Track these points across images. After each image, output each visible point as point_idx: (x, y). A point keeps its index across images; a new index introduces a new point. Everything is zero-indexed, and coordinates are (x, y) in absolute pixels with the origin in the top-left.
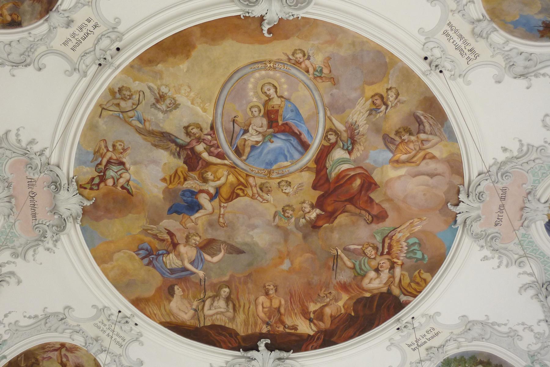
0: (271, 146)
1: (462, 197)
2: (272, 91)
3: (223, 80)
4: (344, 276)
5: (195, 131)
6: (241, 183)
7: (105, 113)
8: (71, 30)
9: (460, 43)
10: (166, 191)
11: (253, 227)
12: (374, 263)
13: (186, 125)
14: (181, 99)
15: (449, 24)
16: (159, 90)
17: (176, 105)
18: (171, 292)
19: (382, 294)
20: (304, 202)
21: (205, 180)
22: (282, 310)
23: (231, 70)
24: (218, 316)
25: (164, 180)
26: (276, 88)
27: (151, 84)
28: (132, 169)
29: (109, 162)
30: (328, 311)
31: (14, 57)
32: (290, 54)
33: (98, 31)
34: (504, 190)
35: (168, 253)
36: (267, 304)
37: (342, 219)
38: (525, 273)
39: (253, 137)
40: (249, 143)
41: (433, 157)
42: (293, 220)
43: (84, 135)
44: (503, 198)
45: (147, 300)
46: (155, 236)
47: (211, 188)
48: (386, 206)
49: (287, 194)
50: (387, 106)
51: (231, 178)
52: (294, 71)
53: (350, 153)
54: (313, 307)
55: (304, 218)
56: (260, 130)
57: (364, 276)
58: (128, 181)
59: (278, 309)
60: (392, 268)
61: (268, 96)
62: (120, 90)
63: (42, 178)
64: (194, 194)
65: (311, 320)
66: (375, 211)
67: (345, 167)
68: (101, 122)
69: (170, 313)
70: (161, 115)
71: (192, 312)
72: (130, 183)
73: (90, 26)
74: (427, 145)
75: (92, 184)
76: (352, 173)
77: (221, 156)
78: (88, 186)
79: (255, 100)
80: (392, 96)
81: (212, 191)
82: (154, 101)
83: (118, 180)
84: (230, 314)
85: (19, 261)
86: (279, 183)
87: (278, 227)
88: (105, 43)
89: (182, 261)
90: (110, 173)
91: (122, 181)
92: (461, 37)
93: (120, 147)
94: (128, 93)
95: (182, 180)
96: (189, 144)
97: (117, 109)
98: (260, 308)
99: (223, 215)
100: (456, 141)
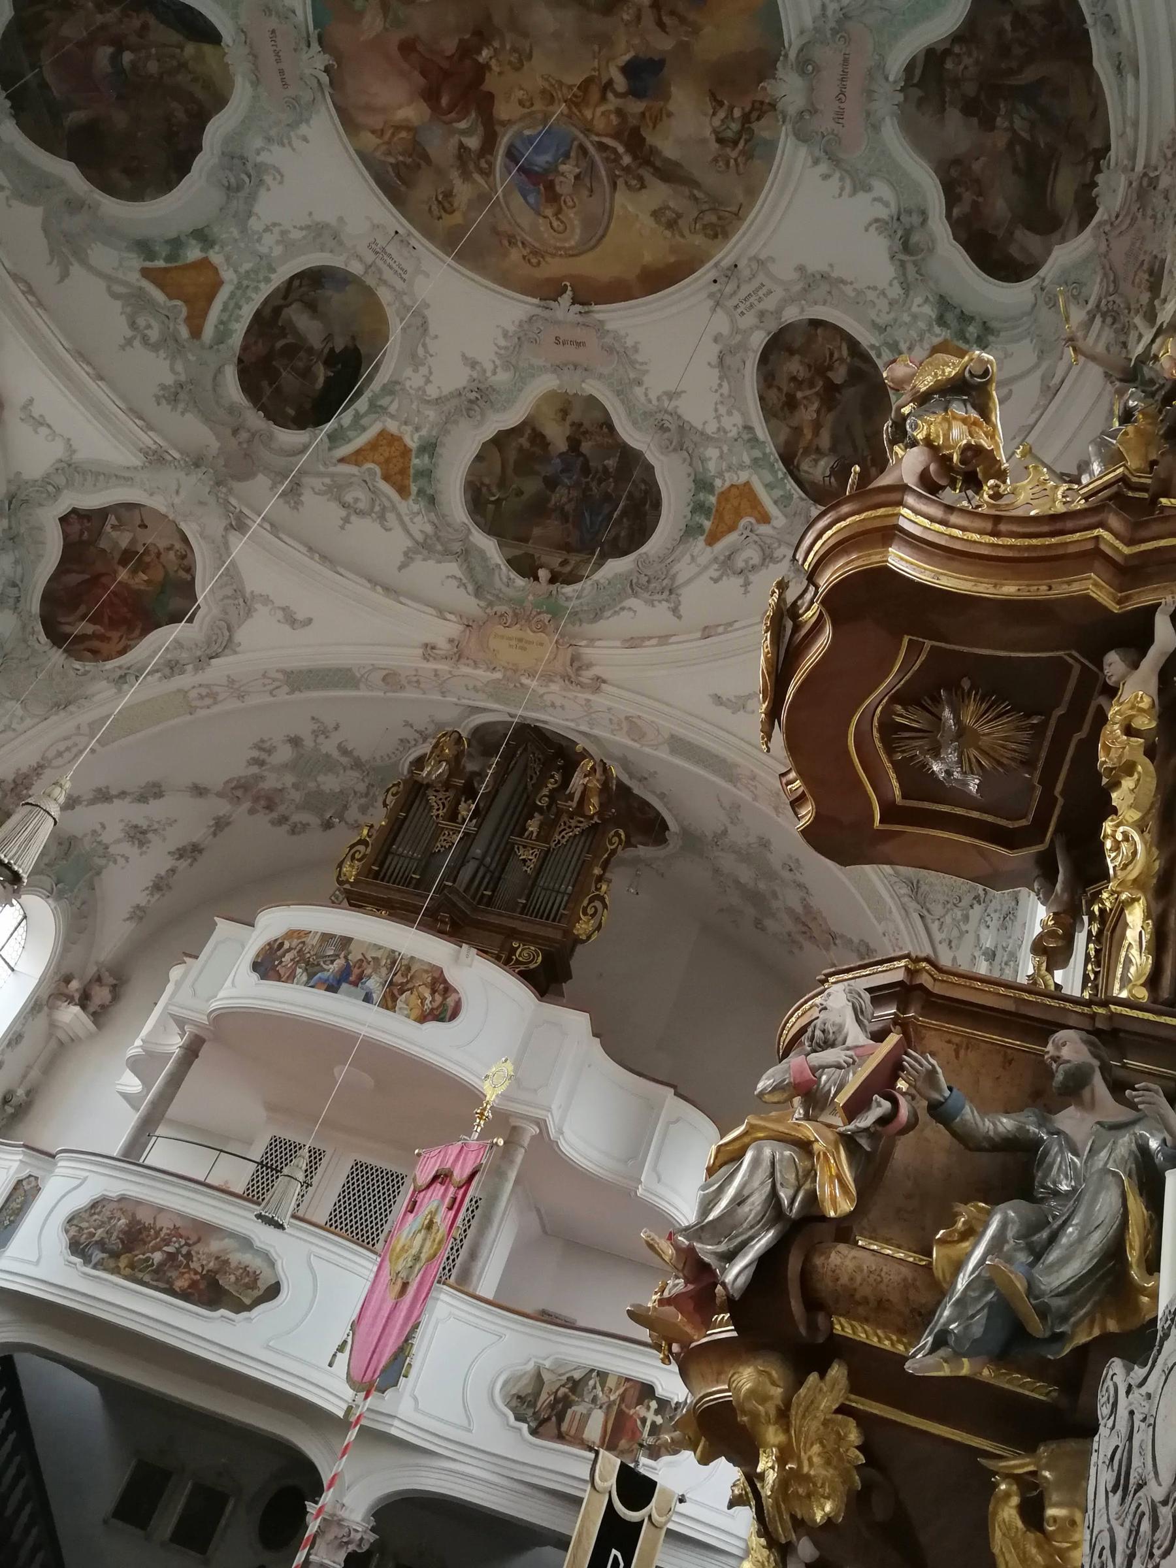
0: (548, 157)
1: (325, 79)
2: (555, 224)
3: (606, 239)
5: (634, 182)
6: (577, 105)
7: (734, 209)
8: (761, 306)
9: (389, 261)
10: (667, 97)
13: (643, 191)
14: (650, 222)
15: (404, 281)
16: (673, 235)
17: (655, 214)
20: (500, 74)
21: (619, 112)
23: (598, 249)
25: (670, 115)
26: (552, 227)
27: (682, 240)
28: (708, 133)
29: (735, 143)
31: (825, 287)
32: (543, 263)
33: (734, 301)
34: (285, 85)
37: (450, 45)
40: (572, 161)
41: (373, 132)
42: (508, 47)
43: (763, 181)
46: (683, 20)
47: (613, 102)
48: (406, 66)
49: (521, 89)
50: (437, 199)
51: (588, 114)
52: (537, 245)
53: (461, 145)
55: (495, 50)
56: (562, 179)
58: (714, 114)
61: (558, 219)
62: (716, 236)
63: (825, 123)
64: (636, 92)
67: (463, 125)
70: (672, 204)
72: (711, 111)
73: (742, 308)
74: (384, 148)
76: (453, 115)
77: (602, 147)
78: (765, 108)
79: (572, 215)
81: (610, 96)
82: (680, 222)
83: (726, 117)
86: (532, 105)
87: (526, 35)
88: (729, 289)
90: (735, 126)
91: (722, 114)
92: (390, 267)
93: (721, 163)
94: (709, 232)
95: (647, 114)
96: (640, 165)
97: (722, 214)
99: (594, 57)
100: (359, 153)
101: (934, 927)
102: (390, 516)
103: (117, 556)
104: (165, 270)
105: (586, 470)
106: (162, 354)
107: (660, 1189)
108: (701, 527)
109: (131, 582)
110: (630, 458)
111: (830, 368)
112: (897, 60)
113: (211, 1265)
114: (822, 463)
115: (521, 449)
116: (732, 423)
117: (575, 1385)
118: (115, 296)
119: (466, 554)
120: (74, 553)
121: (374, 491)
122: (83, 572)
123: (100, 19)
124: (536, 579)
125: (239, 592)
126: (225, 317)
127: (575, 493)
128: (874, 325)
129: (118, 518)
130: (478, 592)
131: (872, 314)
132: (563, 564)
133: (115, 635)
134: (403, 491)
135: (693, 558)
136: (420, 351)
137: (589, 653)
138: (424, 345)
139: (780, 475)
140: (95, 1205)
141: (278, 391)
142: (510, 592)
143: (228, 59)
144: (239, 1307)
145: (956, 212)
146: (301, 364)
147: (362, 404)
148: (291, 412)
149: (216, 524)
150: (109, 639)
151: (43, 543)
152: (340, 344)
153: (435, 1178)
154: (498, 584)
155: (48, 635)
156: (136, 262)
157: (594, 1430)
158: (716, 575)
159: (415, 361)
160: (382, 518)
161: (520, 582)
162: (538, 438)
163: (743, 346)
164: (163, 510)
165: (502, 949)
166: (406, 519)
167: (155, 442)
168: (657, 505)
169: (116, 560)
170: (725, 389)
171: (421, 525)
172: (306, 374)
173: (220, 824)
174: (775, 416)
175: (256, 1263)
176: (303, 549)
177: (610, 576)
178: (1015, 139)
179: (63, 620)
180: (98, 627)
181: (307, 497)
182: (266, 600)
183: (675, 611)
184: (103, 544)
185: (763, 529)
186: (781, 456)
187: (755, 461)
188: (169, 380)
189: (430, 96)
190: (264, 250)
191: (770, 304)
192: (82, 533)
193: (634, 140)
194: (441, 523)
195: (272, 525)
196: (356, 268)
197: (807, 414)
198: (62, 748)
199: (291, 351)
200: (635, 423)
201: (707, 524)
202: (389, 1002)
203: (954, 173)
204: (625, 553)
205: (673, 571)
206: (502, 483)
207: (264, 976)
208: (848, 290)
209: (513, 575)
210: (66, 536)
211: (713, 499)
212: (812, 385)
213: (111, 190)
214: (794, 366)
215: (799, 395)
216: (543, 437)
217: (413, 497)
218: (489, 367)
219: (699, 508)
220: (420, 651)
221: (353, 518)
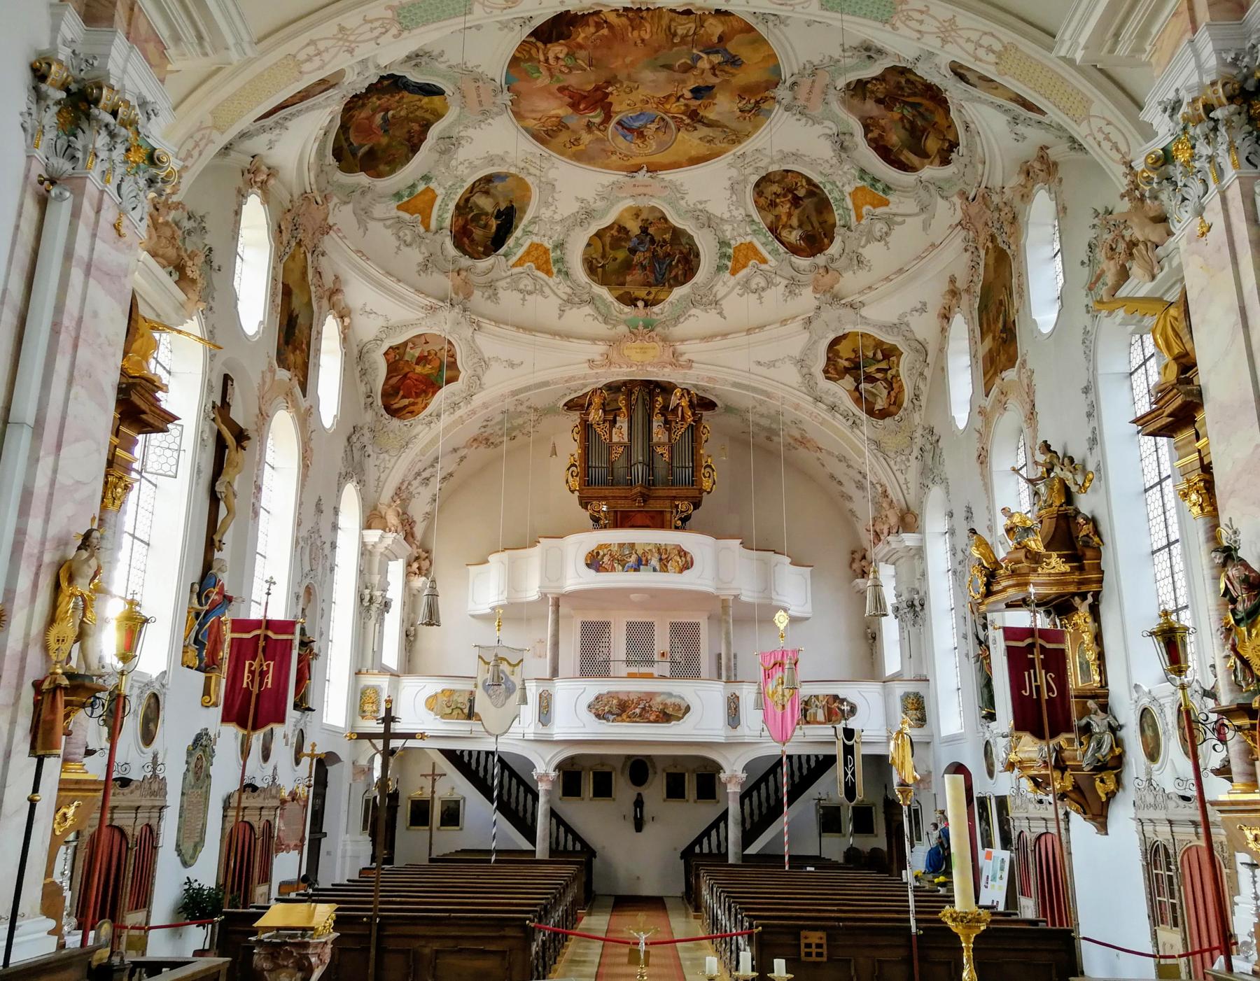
4: (582, 54)
10: (714, 97)
11: (653, 81)
12: (561, 63)
14: (699, 141)
17: (700, 139)
18: (721, 38)
19: (550, 42)
21: (686, 105)
22: (630, 29)
24: (683, 22)
25: (715, 104)
30: (592, 29)
35: (719, 63)
36: (643, 33)
37: (590, 87)
38: (445, 62)
39: (653, 126)
44: (480, 102)
45: (741, 31)
48: (559, 95)
54: (605, 31)
57: (567, 54)
59: (633, 29)
60: (547, 60)
63: (801, 102)
64: (695, 98)
65: (606, 22)
66: (567, 92)
68: (750, 129)
69: (723, 23)
71: (705, 25)
75: (765, 99)
77: (673, 117)
80: (568, 145)
84: (673, 24)
85: (836, 57)
89: (708, 59)
90: (750, 106)
98: (648, 30)
101: (892, 463)
102: (546, 289)
103: (414, 361)
104: (408, 201)
105: (652, 241)
106: (414, 246)
107: (782, 598)
108: (727, 267)
110: (677, 233)
111: (796, 189)
112: (841, 83)
113: (661, 707)
114: (794, 233)
115: (612, 236)
116: (739, 213)
117: (806, 703)
118: (387, 227)
119: (592, 301)
120: (392, 368)
121: (535, 278)
123: (378, 102)
124: (636, 306)
125: (482, 359)
126: (440, 213)
127: (648, 254)
128: (821, 173)
130: (606, 322)
131: (821, 169)
132: (649, 293)
133: (419, 400)
134: (548, 273)
135: (725, 283)
136: (550, 200)
137: (681, 348)
138: (553, 197)
139: (770, 239)
140: (597, 698)
141: (472, 241)
142: (623, 317)
143: (448, 100)
144: (679, 719)
145: (869, 136)
146: (482, 222)
147: (518, 233)
148: (481, 249)
149: (467, 332)
152: (503, 207)
153: (775, 664)
154: (615, 313)
156: (394, 204)
157: (821, 716)
158: (740, 292)
159: (547, 204)
160: (542, 292)
161: (627, 309)
162: (623, 229)
163: (745, 181)
164: (438, 333)
165: (671, 507)
166: (554, 288)
168: (697, 255)
170: (734, 198)
171: (564, 289)
172: (486, 226)
173: (462, 459)
174: (764, 209)
175: (677, 701)
176: (514, 329)
177: (677, 297)
178: (903, 118)
181: (501, 293)
182: (497, 359)
183: (720, 313)
184: (406, 358)
185: (763, 267)
186: (771, 229)
187: (755, 231)
188: (419, 258)
189: (574, 106)
190: (459, 173)
191: (762, 164)
193: (694, 115)
194: (575, 285)
196: (513, 170)
197: (784, 209)
199: (476, 218)
200: (679, 216)
201: (730, 264)
202: (664, 568)
203: (868, 121)
204: (683, 284)
205: (714, 291)
206: (604, 256)
207: (598, 570)
208: (806, 159)
209: (622, 306)
210: (388, 361)
211: (731, 251)
212: (785, 196)
213: (379, 175)
214: (775, 188)
215: (778, 200)
216: (625, 228)
217: (555, 274)
218: (592, 201)
219: (724, 256)
220: (586, 365)
221: (527, 297)
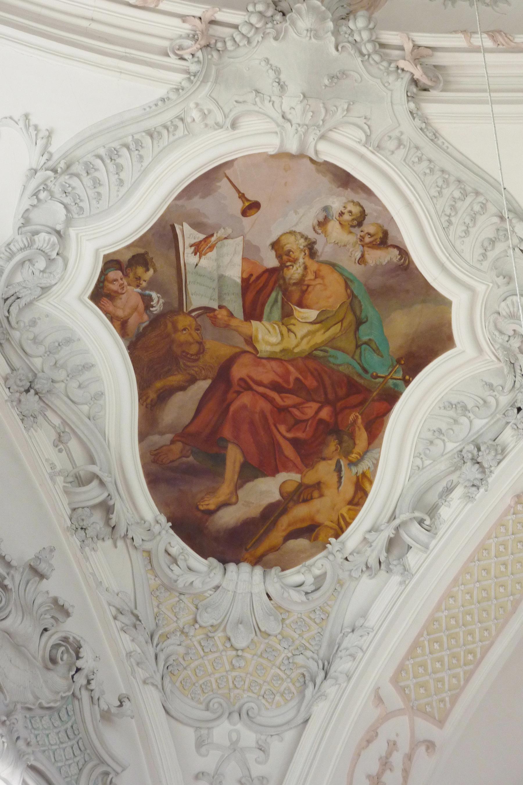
109: (291, 342)
122: (193, 380)
129: (197, 226)
150: (318, 485)
151: (87, 367)
155: (204, 553)
167: (184, 18)
169: (239, 313)
179: (211, 503)
180: (283, 477)
192: (147, 301)
195: (492, 34)
198: (374, 768)
